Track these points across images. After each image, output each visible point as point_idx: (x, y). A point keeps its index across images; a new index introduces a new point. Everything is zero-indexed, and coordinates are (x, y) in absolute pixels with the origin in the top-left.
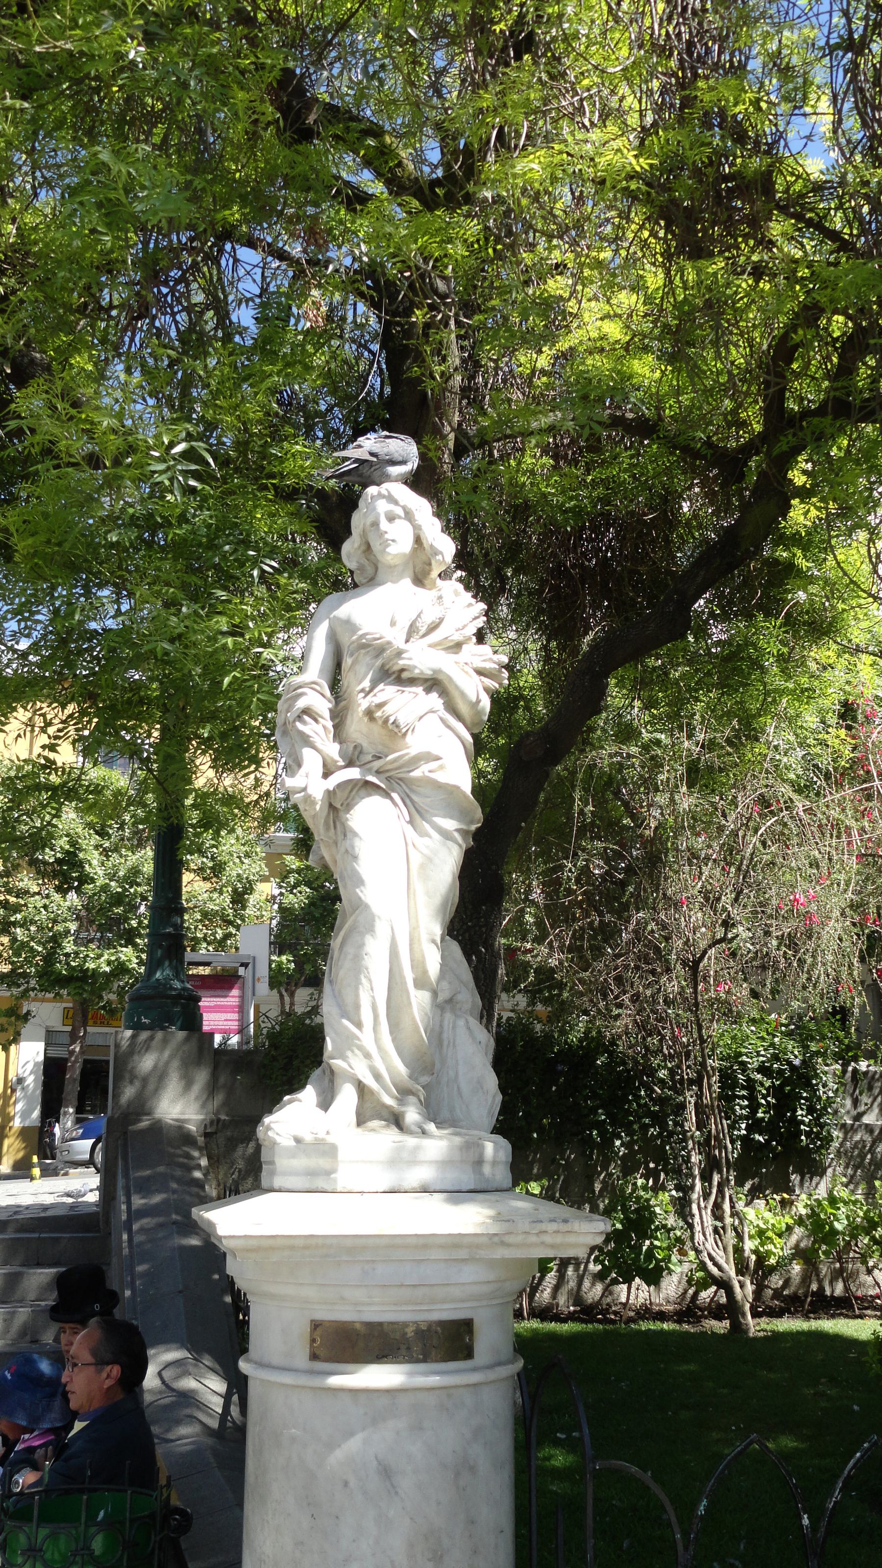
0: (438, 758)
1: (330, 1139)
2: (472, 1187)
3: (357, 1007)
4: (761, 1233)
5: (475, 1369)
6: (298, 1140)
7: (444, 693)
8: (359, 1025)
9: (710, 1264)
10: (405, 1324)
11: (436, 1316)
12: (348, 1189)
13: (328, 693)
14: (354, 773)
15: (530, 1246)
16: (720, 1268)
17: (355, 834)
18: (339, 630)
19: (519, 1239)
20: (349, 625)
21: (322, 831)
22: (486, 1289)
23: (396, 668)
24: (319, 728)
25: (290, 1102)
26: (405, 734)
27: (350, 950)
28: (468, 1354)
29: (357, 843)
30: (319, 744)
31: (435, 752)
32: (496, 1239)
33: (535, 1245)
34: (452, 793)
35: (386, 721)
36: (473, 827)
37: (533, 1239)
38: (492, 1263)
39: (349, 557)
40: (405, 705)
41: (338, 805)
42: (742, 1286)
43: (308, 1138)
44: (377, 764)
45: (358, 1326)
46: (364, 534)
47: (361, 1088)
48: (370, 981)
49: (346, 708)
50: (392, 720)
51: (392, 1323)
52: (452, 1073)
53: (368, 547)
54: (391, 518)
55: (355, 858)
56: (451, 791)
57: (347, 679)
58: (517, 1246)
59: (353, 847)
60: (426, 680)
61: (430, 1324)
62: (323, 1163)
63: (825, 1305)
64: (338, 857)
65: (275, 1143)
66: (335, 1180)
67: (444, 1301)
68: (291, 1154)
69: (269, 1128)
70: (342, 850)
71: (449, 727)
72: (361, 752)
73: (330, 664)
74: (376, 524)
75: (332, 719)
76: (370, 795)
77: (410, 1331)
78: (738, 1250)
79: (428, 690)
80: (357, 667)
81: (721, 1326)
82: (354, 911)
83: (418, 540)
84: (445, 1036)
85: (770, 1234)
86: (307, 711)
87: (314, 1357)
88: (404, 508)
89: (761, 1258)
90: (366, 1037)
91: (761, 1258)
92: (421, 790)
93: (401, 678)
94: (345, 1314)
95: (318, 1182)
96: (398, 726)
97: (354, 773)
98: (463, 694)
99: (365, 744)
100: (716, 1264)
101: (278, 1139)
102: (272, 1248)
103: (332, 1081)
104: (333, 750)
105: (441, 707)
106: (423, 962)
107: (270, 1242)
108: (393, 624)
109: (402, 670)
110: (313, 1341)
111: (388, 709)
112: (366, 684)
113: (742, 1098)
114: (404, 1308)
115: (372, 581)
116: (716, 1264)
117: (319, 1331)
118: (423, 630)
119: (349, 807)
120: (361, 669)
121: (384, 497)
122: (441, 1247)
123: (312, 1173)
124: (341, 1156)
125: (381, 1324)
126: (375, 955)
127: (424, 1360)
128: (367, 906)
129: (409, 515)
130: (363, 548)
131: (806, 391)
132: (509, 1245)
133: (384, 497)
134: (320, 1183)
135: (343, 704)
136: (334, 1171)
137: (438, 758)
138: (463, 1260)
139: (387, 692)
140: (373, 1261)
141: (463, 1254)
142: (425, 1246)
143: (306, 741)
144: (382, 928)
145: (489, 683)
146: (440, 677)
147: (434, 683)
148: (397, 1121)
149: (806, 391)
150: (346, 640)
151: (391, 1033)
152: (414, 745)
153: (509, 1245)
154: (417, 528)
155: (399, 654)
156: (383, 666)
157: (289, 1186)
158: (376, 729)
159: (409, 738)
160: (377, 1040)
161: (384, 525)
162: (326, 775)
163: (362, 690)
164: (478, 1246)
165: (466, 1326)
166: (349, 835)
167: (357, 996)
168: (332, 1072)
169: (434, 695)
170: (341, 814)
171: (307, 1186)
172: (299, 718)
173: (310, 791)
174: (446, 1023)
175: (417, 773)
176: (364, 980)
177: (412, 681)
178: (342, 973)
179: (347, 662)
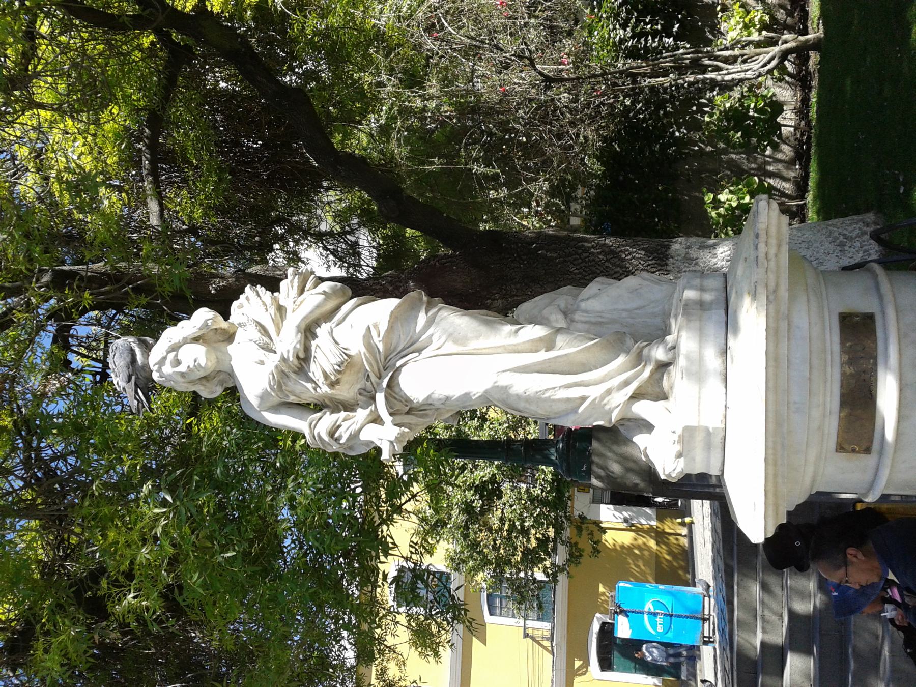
0: (369, 327)
1: (679, 431)
2: (723, 312)
3: (568, 400)
4: (746, 27)
5: (883, 313)
6: (680, 455)
7: (317, 323)
8: (583, 399)
9: (769, 67)
10: (843, 374)
11: (837, 347)
12: (722, 418)
13: (319, 415)
14: (380, 397)
15: (778, 266)
16: (772, 59)
17: (429, 397)
18: (268, 404)
19: (772, 276)
20: (263, 397)
23: (296, 362)
24: (345, 425)
26: (348, 356)
27: (522, 405)
28: (869, 318)
29: (436, 396)
30: (357, 427)
31: (363, 331)
32: (771, 297)
34: (397, 317)
35: (339, 372)
36: (425, 298)
37: (772, 264)
38: (792, 298)
39: (213, 393)
40: (324, 357)
42: (786, 42)
43: (678, 448)
44: (373, 378)
45: (843, 414)
46: (192, 382)
47: (635, 397)
49: (331, 399)
50: (337, 367)
51: (841, 386)
52: (624, 314)
53: (205, 378)
54: (177, 363)
55: (447, 398)
56: (395, 318)
57: (306, 398)
58: (778, 277)
60: (306, 337)
61: (843, 350)
62: (700, 437)
66: (714, 429)
67: (824, 341)
68: (691, 460)
69: (669, 475)
73: (296, 411)
74: (183, 375)
75: (339, 411)
77: (848, 370)
78: (758, 44)
79: (315, 336)
80: (297, 391)
81: (814, 58)
83: (196, 340)
84: (593, 320)
85: (747, 20)
86: (332, 434)
87: (868, 451)
88: (168, 352)
89: (764, 27)
90: (594, 393)
91: (764, 27)
93: (304, 359)
94: (832, 426)
95: (717, 441)
96: (342, 363)
97: (380, 397)
98: (318, 307)
99: (359, 386)
100: (769, 62)
101: (679, 470)
102: (776, 495)
103: (629, 420)
104: (362, 414)
106: (533, 341)
107: (770, 495)
108: (262, 363)
109: (298, 357)
110: (854, 451)
112: (310, 386)
113: (646, 41)
114: (829, 376)
115: (231, 375)
116: (769, 62)
117: (846, 446)
118: (266, 339)
119: (408, 400)
120: (298, 389)
123: (708, 446)
124: (694, 423)
126: (526, 385)
128: (486, 392)
129: (175, 348)
130: (204, 382)
132: (777, 285)
134: (717, 440)
136: (707, 430)
137: (369, 327)
139: (315, 371)
140: (788, 403)
141: (784, 325)
142: (776, 360)
143: (355, 436)
146: (303, 326)
147: (308, 332)
148: (663, 367)
150: (275, 399)
151: (590, 370)
152: (357, 348)
153: (777, 285)
154: (185, 341)
155: (284, 360)
156: (295, 372)
157: (719, 464)
158: (345, 378)
159: (352, 352)
160: (596, 383)
161: (182, 368)
163: (315, 389)
164: (777, 312)
166: (429, 402)
167: (559, 400)
169: (318, 331)
171: (719, 450)
172: (337, 440)
173: (393, 439)
174: (583, 319)
175: (381, 346)
176: (547, 395)
177: (307, 349)
178: (540, 412)
179: (292, 399)
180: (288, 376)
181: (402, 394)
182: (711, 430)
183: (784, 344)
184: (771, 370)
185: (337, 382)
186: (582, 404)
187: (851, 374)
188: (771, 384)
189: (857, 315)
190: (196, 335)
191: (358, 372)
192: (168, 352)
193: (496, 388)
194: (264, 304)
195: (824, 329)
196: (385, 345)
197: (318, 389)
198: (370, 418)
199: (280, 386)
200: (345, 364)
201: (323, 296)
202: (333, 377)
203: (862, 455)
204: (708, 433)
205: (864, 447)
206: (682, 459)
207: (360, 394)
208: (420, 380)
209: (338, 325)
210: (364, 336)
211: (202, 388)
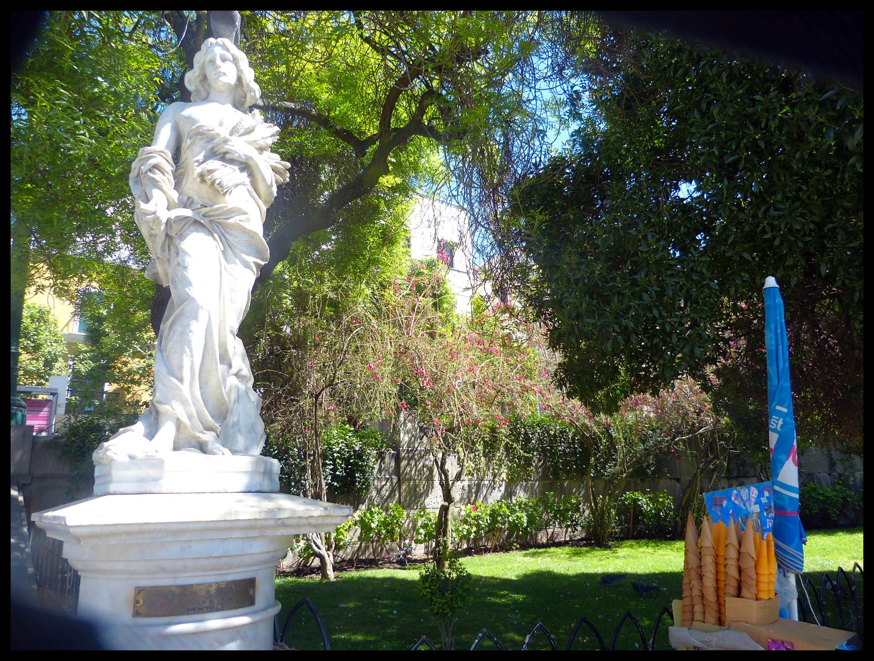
0: (245, 213)
1: (158, 456)
3: (181, 367)
6: (131, 457)
7: (251, 175)
8: (181, 380)
9: (314, 546)
10: (210, 585)
11: (231, 578)
13: (172, 162)
14: (188, 212)
16: (319, 548)
17: (186, 253)
18: (181, 123)
20: (190, 120)
21: (159, 251)
22: (266, 557)
23: (222, 150)
25: (124, 432)
26: (225, 194)
27: (178, 328)
28: (252, 602)
30: (165, 188)
31: (245, 209)
33: (304, 525)
35: (213, 183)
36: (263, 263)
39: (190, 82)
41: (172, 234)
43: (140, 455)
44: (204, 210)
45: (174, 588)
46: (203, 68)
47: (179, 424)
48: (191, 350)
50: (218, 182)
51: (200, 585)
53: (205, 78)
54: (224, 60)
56: (251, 234)
57: (185, 155)
58: (293, 526)
59: (184, 262)
60: (241, 163)
61: (229, 583)
62: (152, 473)
63: (371, 563)
64: (170, 271)
65: (112, 460)
67: (238, 566)
70: (175, 263)
71: (252, 197)
72: (192, 202)
73: (173, 143)
74: (212, 61)
76: (198, 231)
77: (213, 589)
79: (242, 170)
80: (194, 147)
81: (317, 578)
82: (183, 303)
83: (239, 79)
85: (341, 530)
86: (156, 167)
88: (233, 55)
89: (337, 540)
90: (185, 388)
91: (337, 540)
92: (233, 232)
93: (225, 157)
97: (188, 212)
98: (264, 179)
99: (195, 198)
100: (317, 546)
101: (115, 457)
102: (112, 535)
103: (157, 419)
104: (175, 195)
105: (249, 183)
107: (112, 529)
108: (221, 124)
109: (226, 153)
111: (216, 175)
112: (200, 157)
113: (330, 465)
114: (209, 573)
115: (206, 99)
116: (317, 546)
118: (242, 131)
119: (182, 237)
120: (197, 148)
121: (220, 45)
122: (241, 529)
123: (141, 481)
125: (191, 586)
127: (222, 610)
128: (193, 299)
129: (235, 61)
130: (201, 77)
131: (403, 112)
133: (220, 45)
134: (148, 487)
135: (180, 171)
137: (245, 213)
138: (254, 538)
140: (190, 541)
141: (255, 533)
142: (230, 529)
143: (155, 184)
144: (203, 315)
145: (278, 177)
146: (251, 163)
147: (246, 166)
148: (202, 448)
149: (403, 112)
150: (185, 129)
151: (200, 388)
154: (239, 71)
155: (226, 141)
156: (212, 148)
157: (122, 490)
158: (205, 188)
160: (192, 392)
161: (219, 62)
162: (169, 209)
163: (197, 161)
164: (267, 527)
165: (250, 583)
166: (180, 253)
167: (181, 360)
168: (157, 412)
169: (245, 174)
170: (176, 241)
173: (158, 214)
175: (231, 221)
176: (187, 350)
177: (232, 161)
178: (170, 345)
179: (186, 143)
180: (209, 142)
181: (188, 232)
182: (160, 482)
183: (240, 534)
184: (222, 525)
185: (203, 181)
186: (177, 379)
187: (209, 592)
188: (211, 525)
189: (254, 592)
190: (244, 81)
191: (210, 199)
192: (233, 55)
193: (198, 307)
194: (267, 138)
195: (250, 565)
196: (231, 225)
197: (196, 164)
198: (171, 201)
199: (201, 134)
200: (220, 189)
201: (269, 183)
202: (209, 177)
203: (132, 610)
204: (156, 480)
205: (140, 611)
206: (129, 460)
207: (189, 198)
208: (198, 247)
209: (248, 191)
210: (240, 209)
211: (197, 74)
